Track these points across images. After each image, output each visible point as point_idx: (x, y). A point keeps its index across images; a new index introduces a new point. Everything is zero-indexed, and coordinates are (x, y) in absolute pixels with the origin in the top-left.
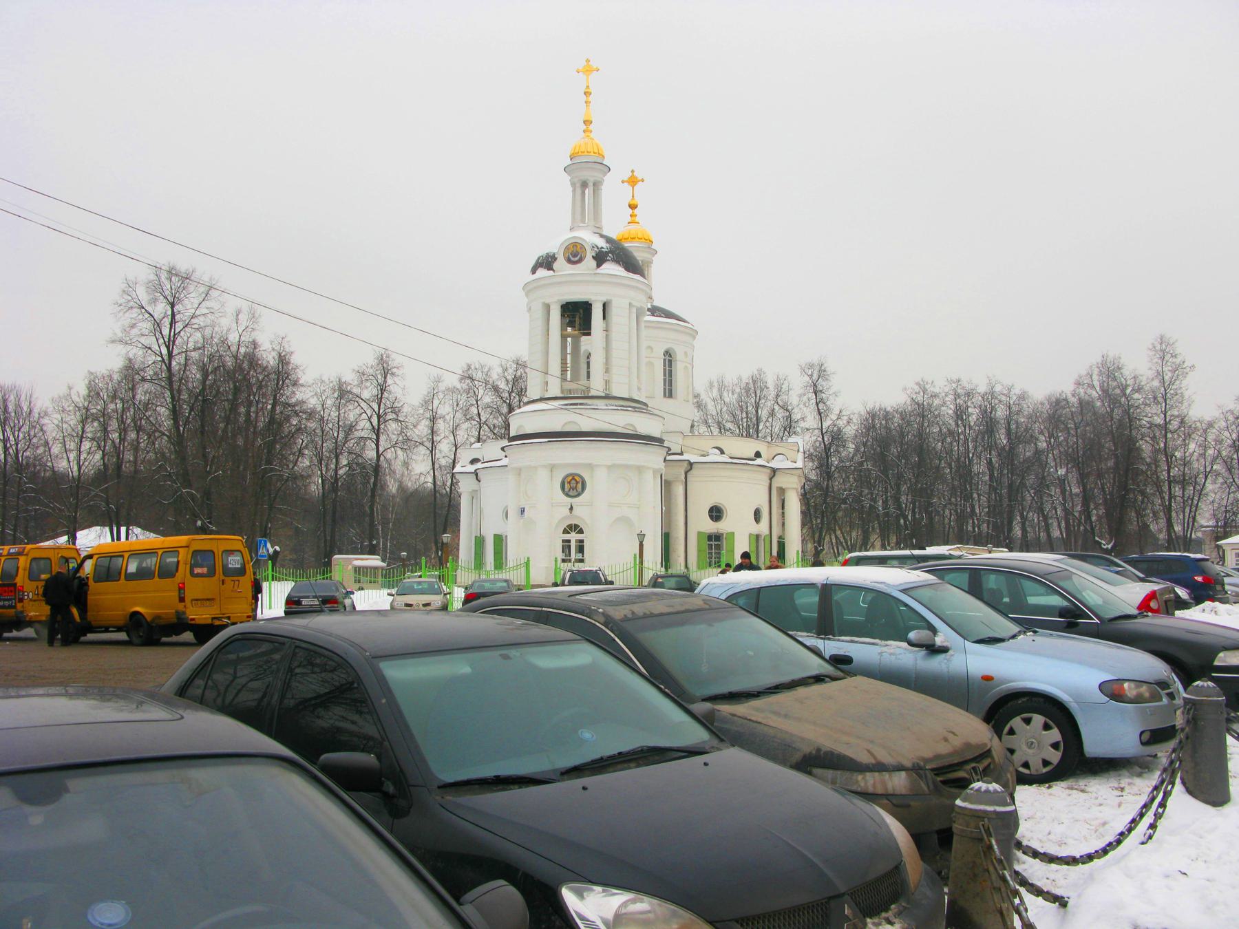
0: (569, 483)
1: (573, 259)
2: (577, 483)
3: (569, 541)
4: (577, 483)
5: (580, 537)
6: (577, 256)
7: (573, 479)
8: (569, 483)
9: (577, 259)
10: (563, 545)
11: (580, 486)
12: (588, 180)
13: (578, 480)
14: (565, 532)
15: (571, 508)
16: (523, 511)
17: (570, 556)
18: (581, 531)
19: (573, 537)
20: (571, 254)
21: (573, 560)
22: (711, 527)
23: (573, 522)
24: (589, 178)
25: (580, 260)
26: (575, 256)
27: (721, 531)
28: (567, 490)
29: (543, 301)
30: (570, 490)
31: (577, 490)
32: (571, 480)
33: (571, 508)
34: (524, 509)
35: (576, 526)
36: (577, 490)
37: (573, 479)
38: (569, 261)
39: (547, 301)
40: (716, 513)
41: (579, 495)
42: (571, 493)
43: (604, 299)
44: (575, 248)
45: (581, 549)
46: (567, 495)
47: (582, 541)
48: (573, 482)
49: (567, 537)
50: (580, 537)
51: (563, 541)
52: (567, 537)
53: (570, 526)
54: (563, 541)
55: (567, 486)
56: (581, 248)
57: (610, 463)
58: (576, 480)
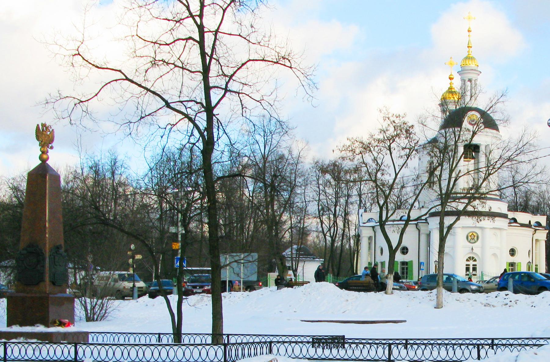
1: (473, 123)
2: (474, 236)
3: (469, 265)
4: (474, 236)
5: (475, 263)
7: (472, 234)
10: (466, 267)
11: (476, 238)
14: (467, 260)
15: (472, 249)
18: (475, 260)
19: (471, 263)
33: (472, 249)
35: (473, 258)
37: (472, 234)
40: (512, 252)
41: (475, 242)
42: (472, 241)
45: (474, 269)
46: (470, 242)
47: (475, 265)
52: (468, 263)
53: (470, 258)
54: (467, 265)
55: (469, 238)
58: (474, 235)
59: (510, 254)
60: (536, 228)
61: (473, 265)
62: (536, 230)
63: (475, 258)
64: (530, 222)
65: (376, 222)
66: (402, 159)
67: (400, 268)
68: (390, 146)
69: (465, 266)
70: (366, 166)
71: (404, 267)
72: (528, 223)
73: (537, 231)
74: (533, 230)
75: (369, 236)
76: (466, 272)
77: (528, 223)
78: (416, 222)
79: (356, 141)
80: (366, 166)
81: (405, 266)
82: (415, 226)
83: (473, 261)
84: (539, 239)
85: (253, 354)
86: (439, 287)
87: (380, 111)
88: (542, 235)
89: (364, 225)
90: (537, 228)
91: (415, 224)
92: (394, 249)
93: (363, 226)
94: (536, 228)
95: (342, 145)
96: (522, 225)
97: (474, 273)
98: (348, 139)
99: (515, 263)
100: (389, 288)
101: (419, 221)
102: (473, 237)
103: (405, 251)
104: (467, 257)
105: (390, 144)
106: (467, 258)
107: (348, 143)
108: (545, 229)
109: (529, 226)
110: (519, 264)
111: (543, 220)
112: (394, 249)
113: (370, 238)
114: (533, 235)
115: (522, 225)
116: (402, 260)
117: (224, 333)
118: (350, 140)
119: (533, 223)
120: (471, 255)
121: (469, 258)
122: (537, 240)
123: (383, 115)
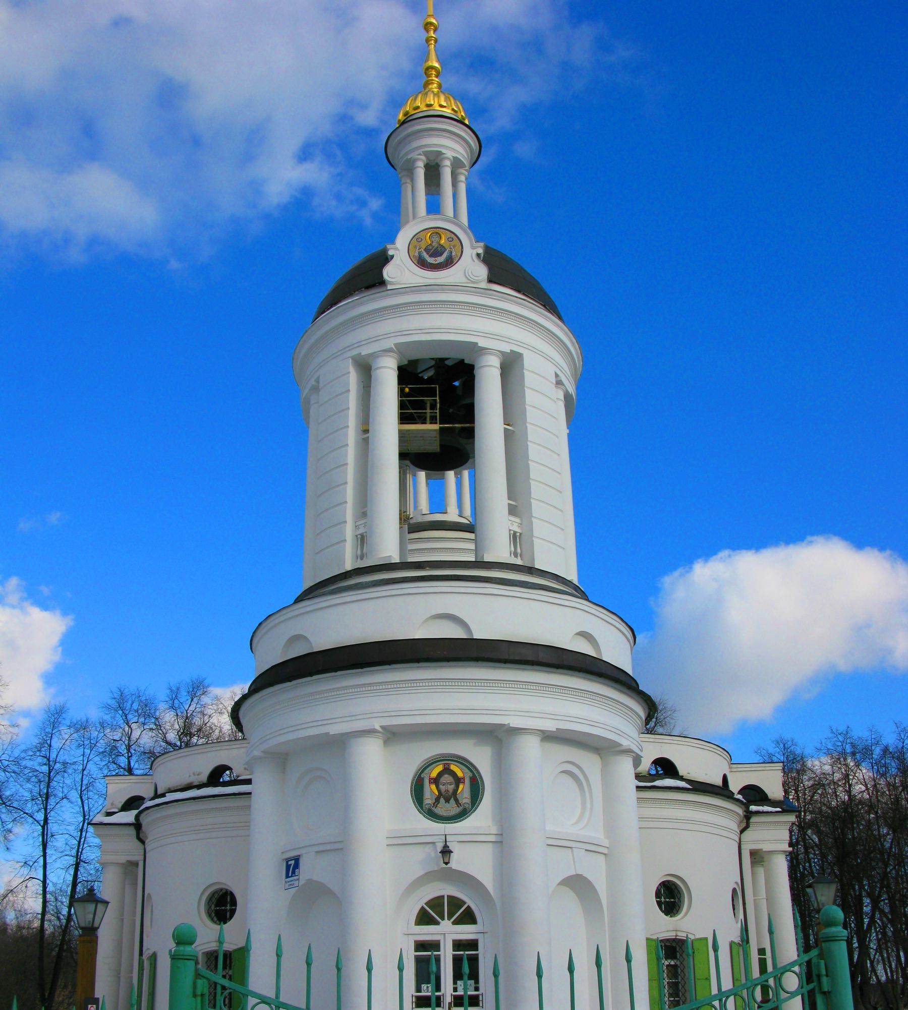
0: (436, 781)
1: (431, 260)
3: (434, 946)
4: (458, 781)
5: (466, 932)
6: (441, 254)
7: (447, 770)
8: (436, 781)
9: (441, 259)
11: (464, 790)
12: (440, 153)
13: (460, 774)
14: (424, 918)
16: (292, 867)
17: (438, 988)
20: (426, 250)
21: (448, 999)
24: (444, 151)
25: (449, 263)
26: (436, 253)
27: (682, 935)
28: (428, 799)
29: (355, 352)
30: (437, 800)
31: (457, 801)
32: (440, 774)
33: (446, 852)
34: (297, 860)
35: (455, 903)
36: (457, 801)
37: (447, 770)
38: (422, 263)
39: (365, 351)
41: (463, 814)
42: (444, 809)
43: (507, 348)
44: (435, 239)
46: (431, 815)
47: (473, 945)
48: (447, 778)
49: (428, 933)
50: (466, 932)
51: (421, 946)
52: (428, 933)
53: (436, 903)
54: (421, 946)
55: (430, 791)
56: (450, 240)
57: (550, 726)
58: (453, 774)
59: (659, 904)
61: (458, 945)
62: (748, 815)
63: (469, 902)
64: (725, 778)
72: (719, 782)
73: (754, 819)
75: (123, 859)
76: (418, 989)
77: (719, 782)
83: (455, 923)
84: (766, 847)
90: (753, 808)
102: (451, 788)
106: (422, 903)
109: (722, 790)
110: (695, 944)
115: (699, 787)
119: (735, 786)
120: (447, 890)
121: (430, 903)
122: (754, 854)
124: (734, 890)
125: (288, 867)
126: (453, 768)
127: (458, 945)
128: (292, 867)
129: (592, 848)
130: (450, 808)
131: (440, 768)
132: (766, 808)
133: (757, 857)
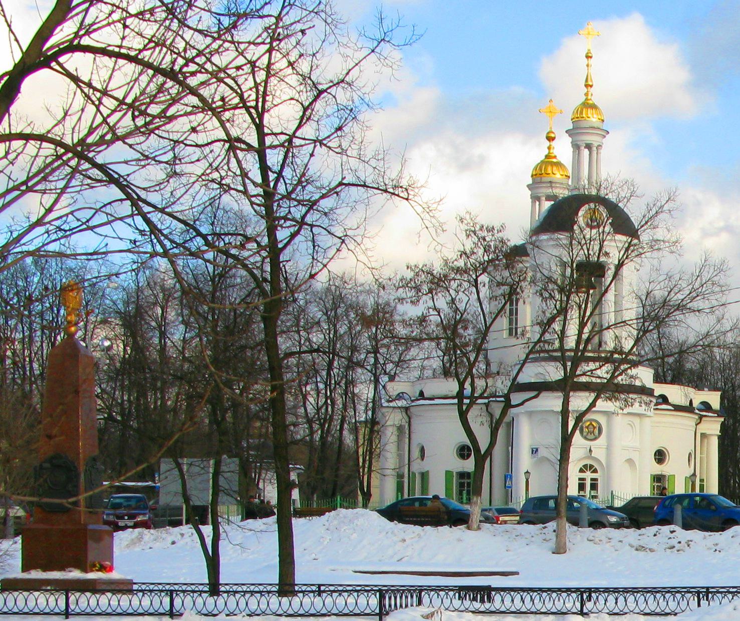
0: (587, 427)
3: (584, 479)
4: (594, 428)
5: (594, 476)
7: (591, 424)
8: (587, 427)
11: (596, 431)
14: (581, 471)
18: (595, 471)
19: (588, 475)
22: (658, 469)
23: (589, 462)
27: (664, 473)
28: (585, 434)
33: (590, 451)
34: (537, 450)
35: (591, 466)
40: (660, 456)
42: (590, 437)
45: (594, 487)
46: (586, 438)
47: (596, 480)
48: (591, 426)
49: (582, 475)
50: (594, 476)
51: (580, 479)
52: (582, 475)
53: (585, 466)
54: (580, 479)
59: (655, 459)
60: (701, 413)
61: (592, 479)
62: (701, 417)
64: (691, 402)
65: (413, 399)
66: (497, 303)
67: (456, 483)
68: (476, 281)
69: (577, 482)
70: (439, 315)
71: (464, 483)
73: (704, 419)
74: (697, 417)
78: (486, 401)
79: (422, 270)
80: (439, 315)
81: (466, 481)
82: (484, 408)
84: (708, 432)
85: (404, 606)
86: (561, 518)
87: (462, 220)
88: (713, 427)
89: (391, 404)
90: (704, 413)
91: (485, 403)
92: (482, 453)
93: (388, 407)
94: (701, 413)
95: (399, 277)
96: (678, 408)
97: (593, 493)
98: (408, 268)
99: (664, 476)
100: (474, 520)
101: (491, 399)
103: (466, 453)
104: (580, 465)
105: (477, 277)
107: (409, 275)
108: (719, 416)
110: (670, 477)
111: (714, 399)
112: (482, 453)
113: (400, 429)
114: (696, 425)
115: (678, 408)
116: (460, 470)
117: (296, 583)
118: (412, 270)
119: (696, 404)
120: (589, 462)
121: (584, 466)
122: (702, 434)
123: (466, 228)
124: (690, 454)
125: (533, 451)
126: (593, 423)
127: (592, 479)
128: (535, 451)
129: (635, 449)
130: (592, 437)
131: (588, 423)
132: (710, 414)
133: (703, 436)
